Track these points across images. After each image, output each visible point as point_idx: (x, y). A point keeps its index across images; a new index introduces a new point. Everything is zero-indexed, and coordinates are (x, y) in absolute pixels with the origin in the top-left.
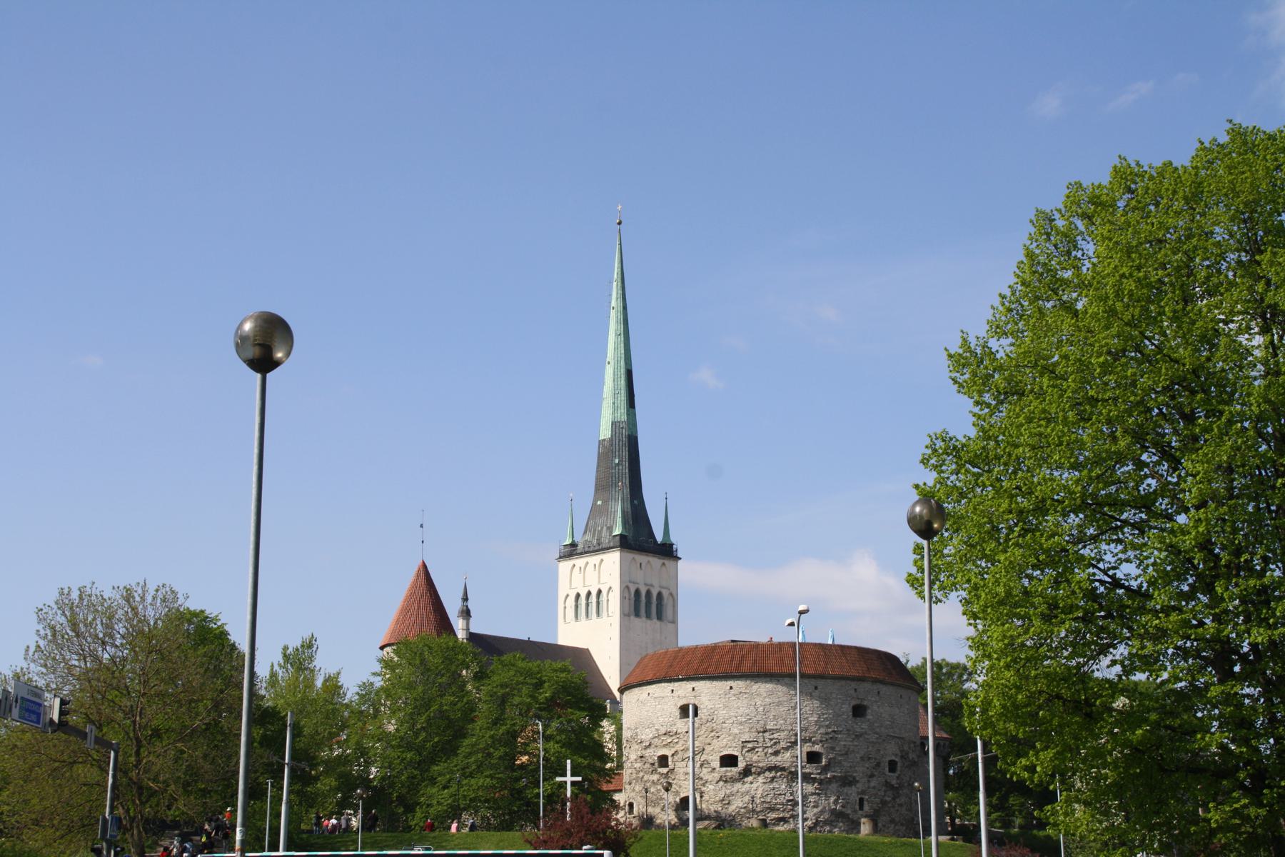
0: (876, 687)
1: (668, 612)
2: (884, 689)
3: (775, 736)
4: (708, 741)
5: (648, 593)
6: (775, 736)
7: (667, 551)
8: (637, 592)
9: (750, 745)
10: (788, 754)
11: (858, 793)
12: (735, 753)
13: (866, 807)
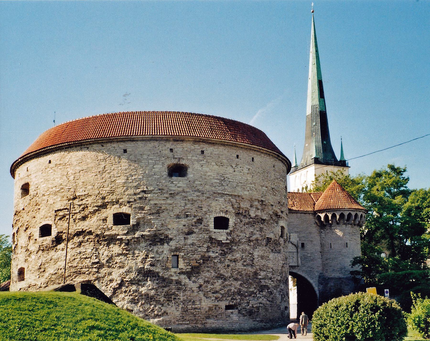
0: (198, 147)
2: (209, 149)
3: (84, 202)
6: (84, 202)
9: (61, 213)
10: (95, 218)
13: (182, 265)
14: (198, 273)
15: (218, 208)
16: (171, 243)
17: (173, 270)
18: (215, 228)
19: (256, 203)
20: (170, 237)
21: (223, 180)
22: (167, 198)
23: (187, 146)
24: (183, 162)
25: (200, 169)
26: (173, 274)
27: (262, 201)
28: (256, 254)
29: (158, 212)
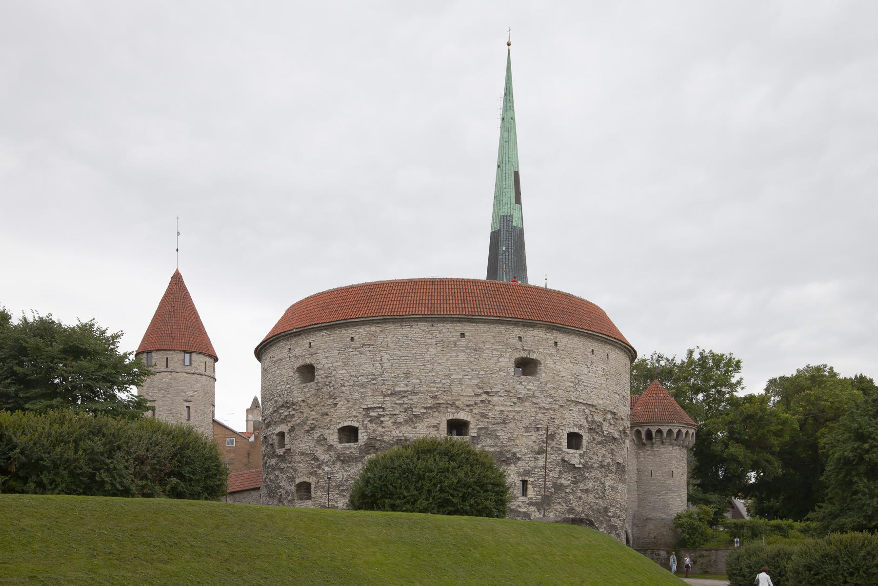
2: (564, 340)
4: (324, 410)
11: (519, 474)
12: (356, 424)
13: (531, 493)
14: (549, 505)
15: (574, 420)
16: (520, 463)
17: (522, 499)
18: (568, 448)
19: (609, 416)
20: (518, 456)
21: (577, 382)
22: (515, 403)
23: (539, 333)
24: (534, 356)
25: (553, 366)
26: (520, 504)
27: (614, 414)
28: (607, 484)
29: (504, 422)
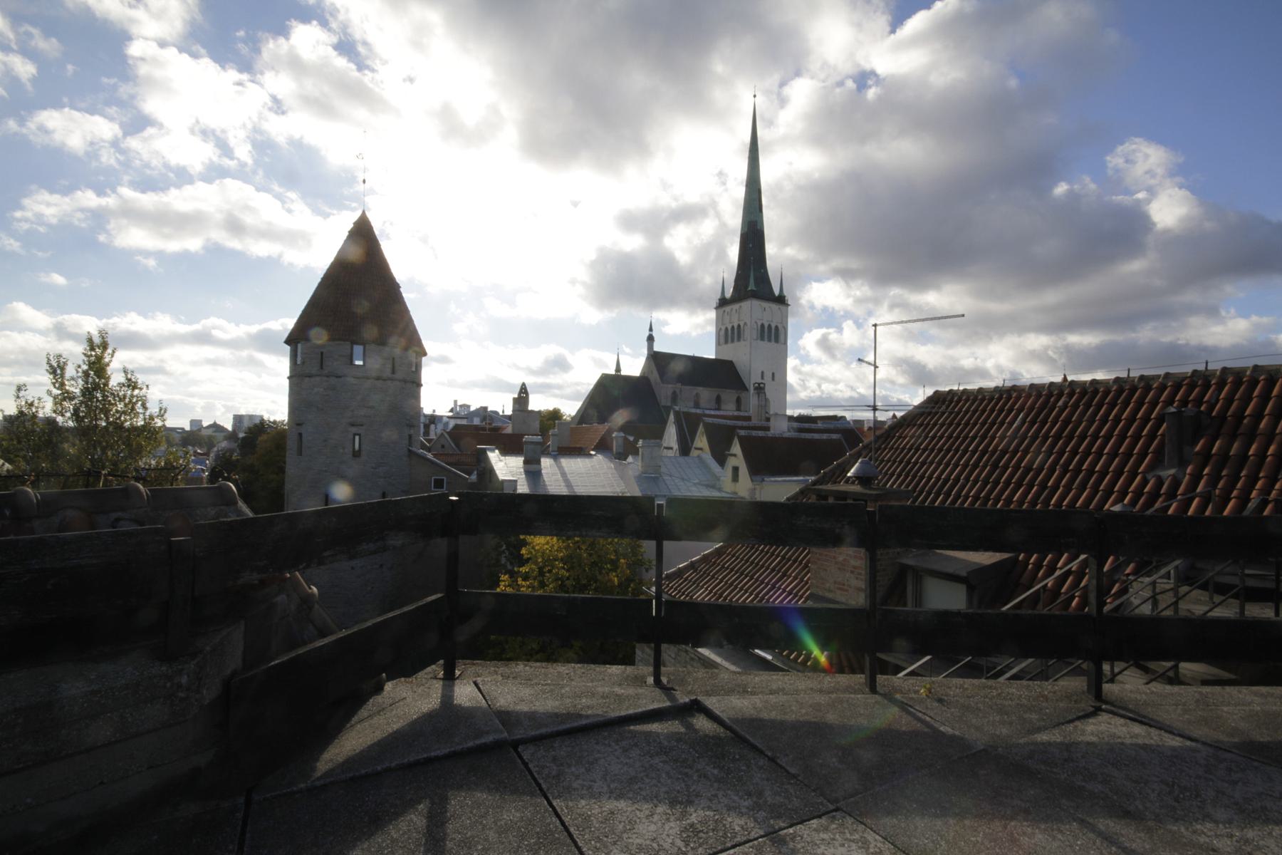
1: (782, 337)
5: (770, 326)
7: (781, 300)
8: (762, 326)
